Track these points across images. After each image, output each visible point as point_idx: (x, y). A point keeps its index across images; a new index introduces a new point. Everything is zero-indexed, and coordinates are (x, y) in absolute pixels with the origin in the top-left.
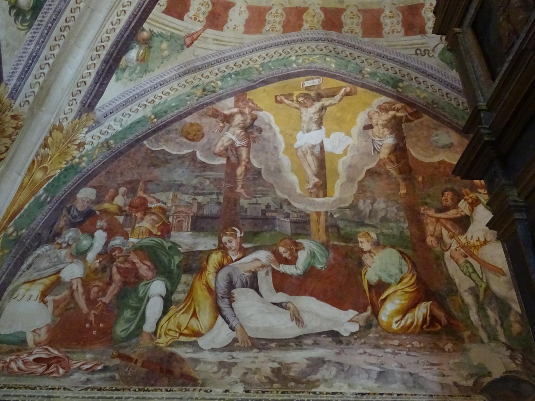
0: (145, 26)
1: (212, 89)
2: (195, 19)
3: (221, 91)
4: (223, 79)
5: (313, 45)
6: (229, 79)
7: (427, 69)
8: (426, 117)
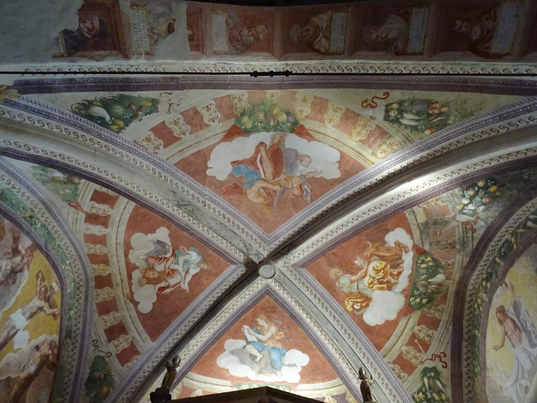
0: (83, 180)
1: (33, 222)
2: (93, 207)
3: (33, 230)
4: (43, 226)
5: (81, 272)
6: (44, 230)
7: (84, 352)
8: (53, 373)
